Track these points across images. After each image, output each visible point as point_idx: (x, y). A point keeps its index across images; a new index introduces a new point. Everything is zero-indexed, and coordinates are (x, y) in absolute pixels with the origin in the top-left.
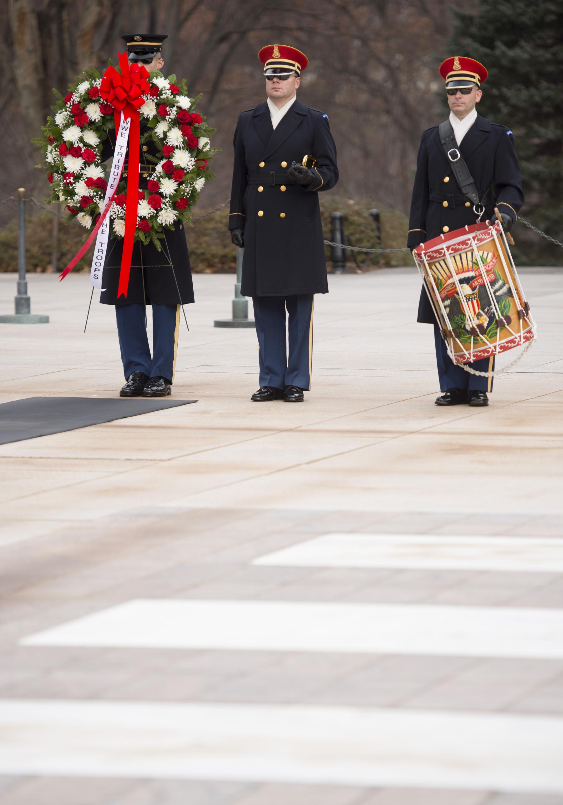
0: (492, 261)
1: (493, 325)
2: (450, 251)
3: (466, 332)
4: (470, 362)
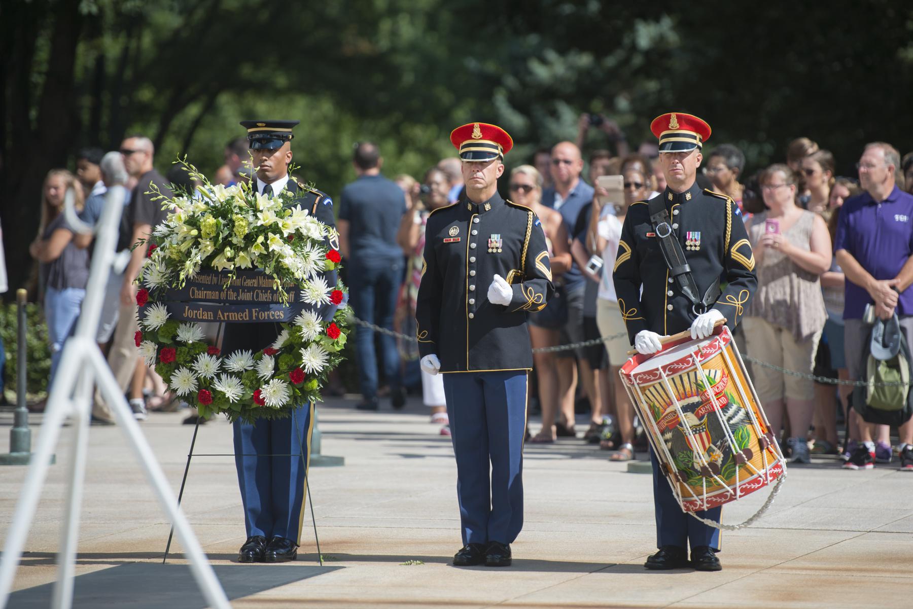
1: (729, 463)
3: (695, 473)
4: (703, 510)
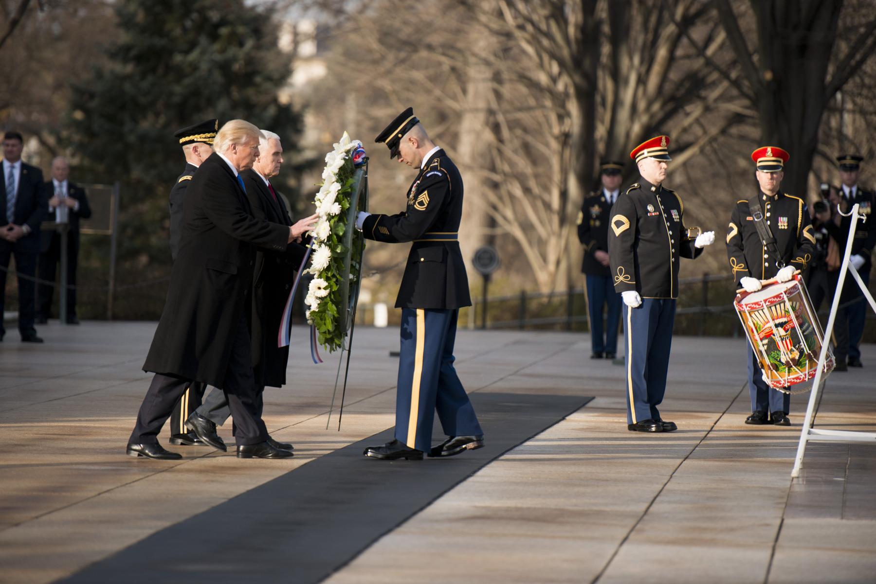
0: (799, 308)
2: (767, 303)
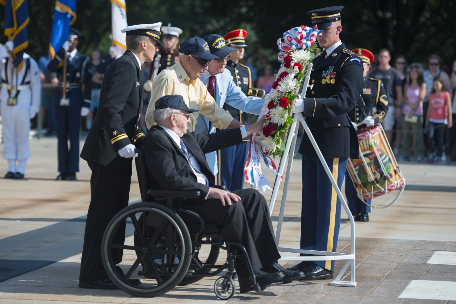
0: (379, 144)
